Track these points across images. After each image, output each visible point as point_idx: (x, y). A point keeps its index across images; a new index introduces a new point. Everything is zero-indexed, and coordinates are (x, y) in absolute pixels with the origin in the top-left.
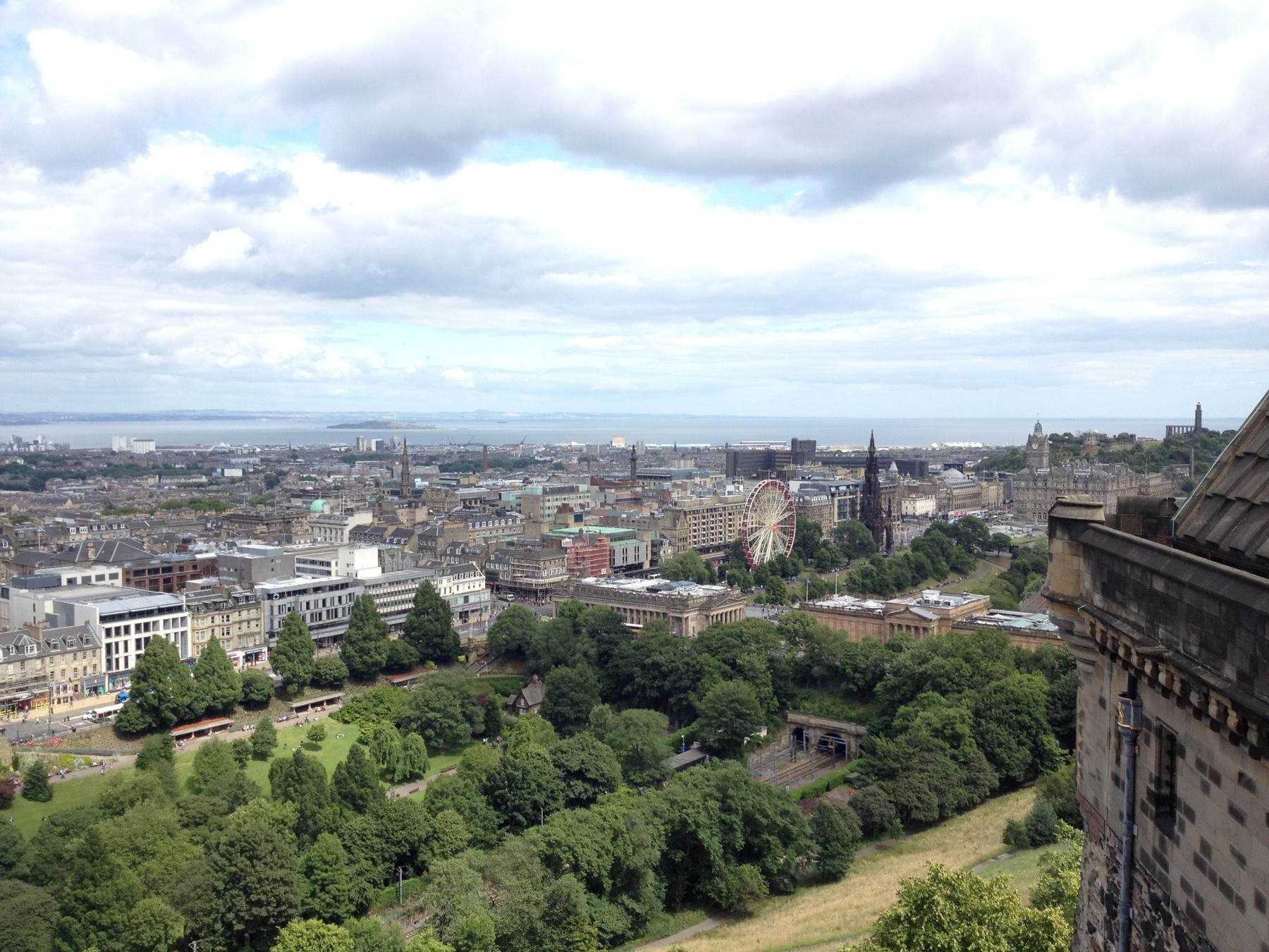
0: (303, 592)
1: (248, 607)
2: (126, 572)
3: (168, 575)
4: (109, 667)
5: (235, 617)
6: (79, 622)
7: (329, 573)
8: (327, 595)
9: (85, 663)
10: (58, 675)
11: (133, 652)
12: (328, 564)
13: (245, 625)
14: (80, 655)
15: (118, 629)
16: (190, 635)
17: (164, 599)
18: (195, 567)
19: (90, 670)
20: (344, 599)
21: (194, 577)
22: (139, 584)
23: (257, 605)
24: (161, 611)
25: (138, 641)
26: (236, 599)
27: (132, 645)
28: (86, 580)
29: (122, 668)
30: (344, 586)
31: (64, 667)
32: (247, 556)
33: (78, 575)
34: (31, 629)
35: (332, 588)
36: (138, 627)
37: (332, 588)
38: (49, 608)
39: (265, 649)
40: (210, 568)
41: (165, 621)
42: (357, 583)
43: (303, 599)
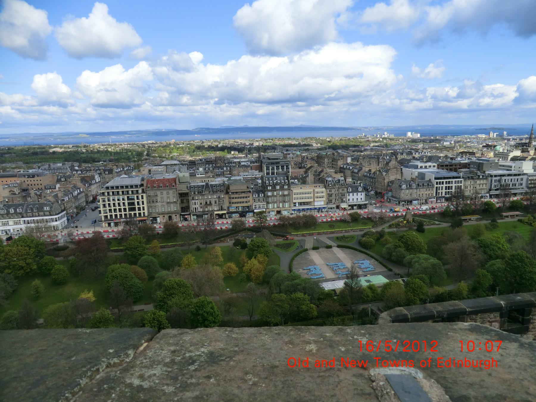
0: (504, 175)
1: (483, 179)
2: (438, 165)
3: (451, 167)
4: (436, 195)
5: (478, 182)
6: (427, 179)
7: (511, 170)
8: (513, 178)
9: (429, 192)
10: (421, 195)
11: (444, 191)
12: (511, 167)
13: (481, 185)
14: (428, 189)
15: (440, 182)
16: (469, 187)
17: (454, 174)
18: (460, 165)
19: (430, 195)
20: (519, 180)
21: (459, 169)
22: (443, 169)
23: (486, 178)
24: (454, 178)
25: (446, 187)
26: (479, 176)
27: (444, 188)
28: (426, 167)
29: (440, 195)
30: (519, 175)
31: (424, 192)
32: (481, 162)
33: (423, 165)
34: (413, 180)
35: (515, 175)
36: (446, 182)
37: (515, 175)
38: (416, 174)
39: (488, 195)
40: (465, 166)
41: (455, 181)
42: (524, 174)
43: (504, 178)
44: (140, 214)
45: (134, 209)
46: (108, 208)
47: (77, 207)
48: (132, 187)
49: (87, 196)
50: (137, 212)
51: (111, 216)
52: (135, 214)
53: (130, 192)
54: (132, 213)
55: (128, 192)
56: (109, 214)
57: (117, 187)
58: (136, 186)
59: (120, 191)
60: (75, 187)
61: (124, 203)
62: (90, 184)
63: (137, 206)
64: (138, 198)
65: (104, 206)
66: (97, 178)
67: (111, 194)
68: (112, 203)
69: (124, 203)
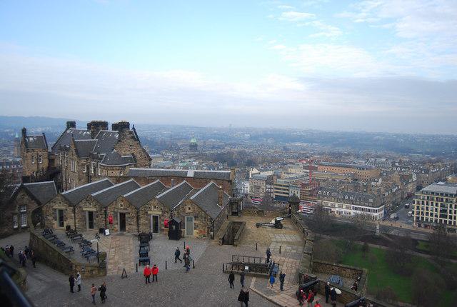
44: (450, 222)
45: (446, 217)
46: (421, 211)
47: (393, 203)
48: (447, 195)
49: (403, 193)
50: (448, 220)
51: (423, 218)
52: (445, 221)
53: (445, 200)
54: (443, 219)
55: (442, 199)
56: (420, 216)
57: (433, 193)
58: (451, 195)
59: (435, 197)
60: (395, 184)
61: (436, 209)
62: (408, 183)
63: (449, 214)
64: (451, 207)
65: (418, 208)
66: (414, 178)
67: (426, 198)
68: (426, 206)
69: (436, 209)
